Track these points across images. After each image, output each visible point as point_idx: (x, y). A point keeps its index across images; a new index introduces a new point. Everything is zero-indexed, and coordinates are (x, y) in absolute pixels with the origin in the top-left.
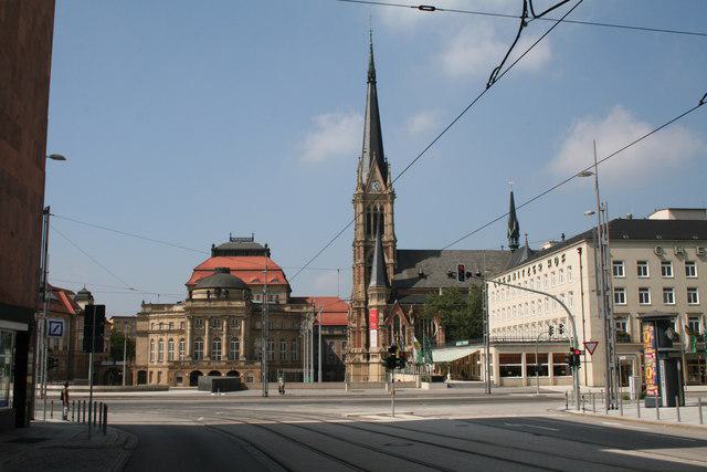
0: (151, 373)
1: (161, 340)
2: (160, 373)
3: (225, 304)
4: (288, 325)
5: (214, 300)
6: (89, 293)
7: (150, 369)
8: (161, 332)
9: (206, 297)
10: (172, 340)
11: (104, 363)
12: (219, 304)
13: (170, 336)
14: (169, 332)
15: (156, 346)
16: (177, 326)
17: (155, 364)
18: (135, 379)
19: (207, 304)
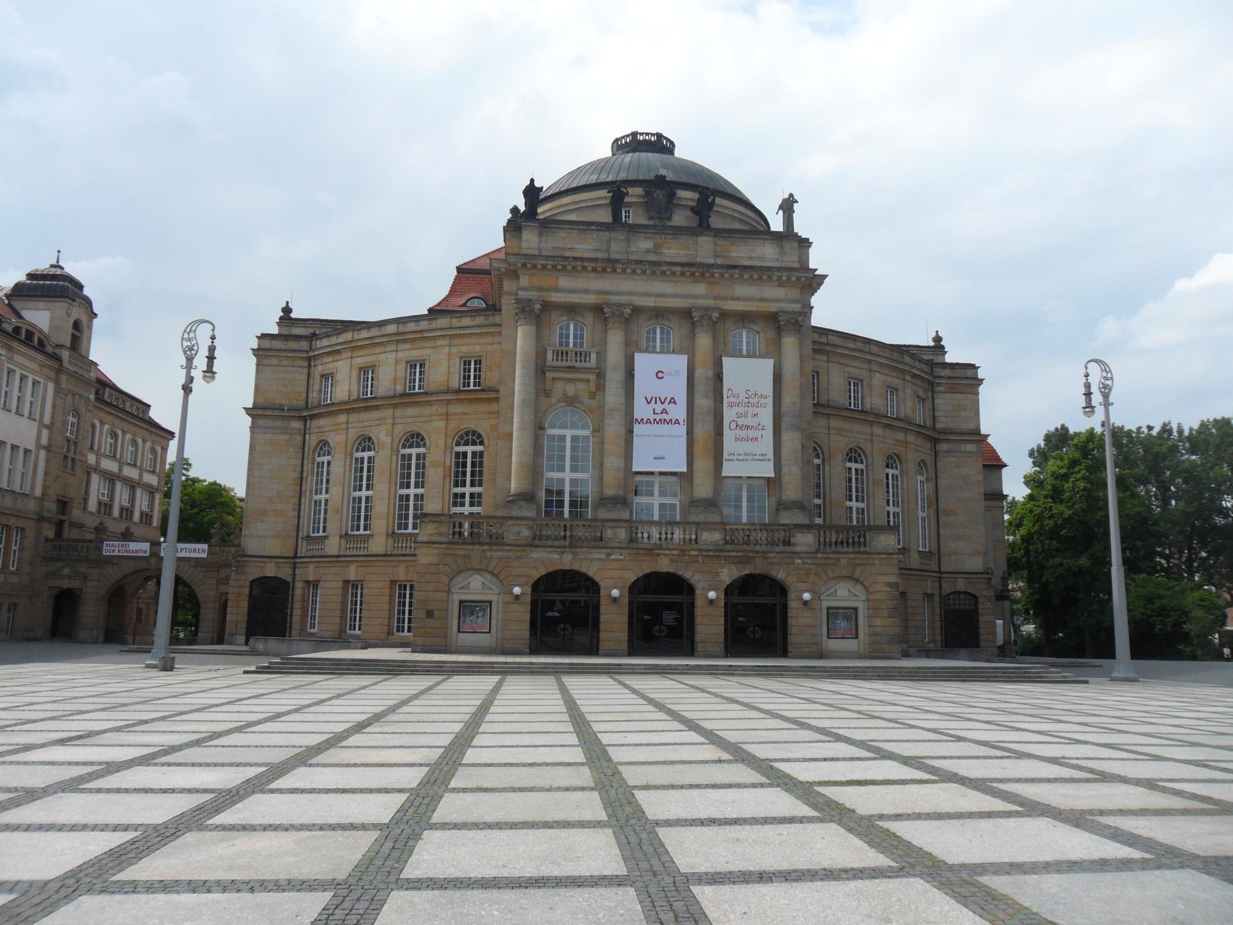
0: (315, 584)
1: (366, 442)
2: (352, 587)
3: (704, 249)
4: (907, 405)
5: (634, 229)
6: (80, 287)
7: (311, 573)
8: (363, 404)
9: (605, 216)
10: (415, 439)
11: (112, 548)
12: (674, 251)
13: (409, 419)
14: (405, 399)
15: (339, 467)
16: (443, 368)
17: (333, 546)
18: (238, 613)
19: (617, 246)
